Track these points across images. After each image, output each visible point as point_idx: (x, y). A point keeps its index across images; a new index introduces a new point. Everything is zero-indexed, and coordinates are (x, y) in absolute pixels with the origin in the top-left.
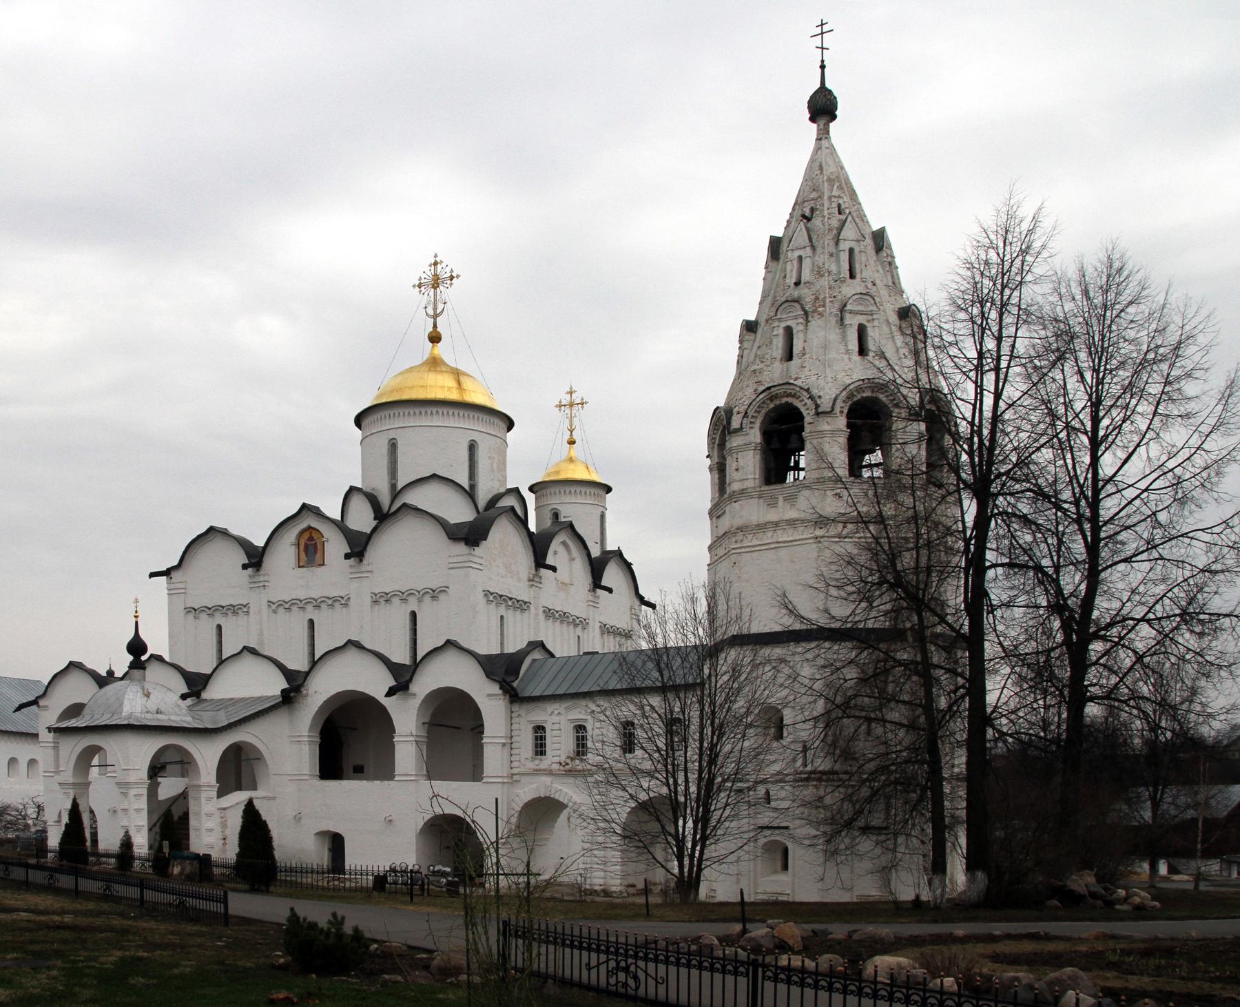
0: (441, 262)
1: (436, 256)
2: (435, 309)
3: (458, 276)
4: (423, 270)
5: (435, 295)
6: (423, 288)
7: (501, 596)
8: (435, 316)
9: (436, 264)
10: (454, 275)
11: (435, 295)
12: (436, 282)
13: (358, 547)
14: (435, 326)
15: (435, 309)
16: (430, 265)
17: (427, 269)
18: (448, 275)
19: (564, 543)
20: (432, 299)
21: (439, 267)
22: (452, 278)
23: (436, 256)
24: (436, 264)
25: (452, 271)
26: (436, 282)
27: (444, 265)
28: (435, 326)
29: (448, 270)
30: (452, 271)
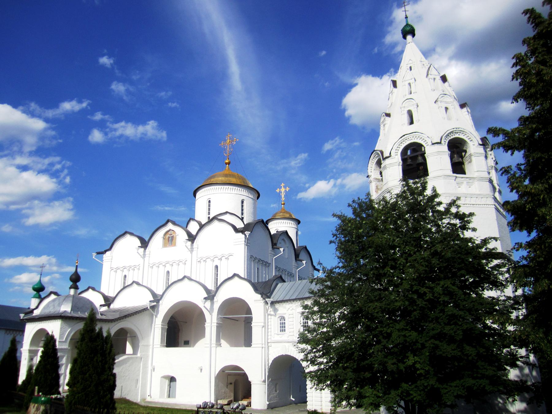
13: (192, 238)
19: (283, 239)
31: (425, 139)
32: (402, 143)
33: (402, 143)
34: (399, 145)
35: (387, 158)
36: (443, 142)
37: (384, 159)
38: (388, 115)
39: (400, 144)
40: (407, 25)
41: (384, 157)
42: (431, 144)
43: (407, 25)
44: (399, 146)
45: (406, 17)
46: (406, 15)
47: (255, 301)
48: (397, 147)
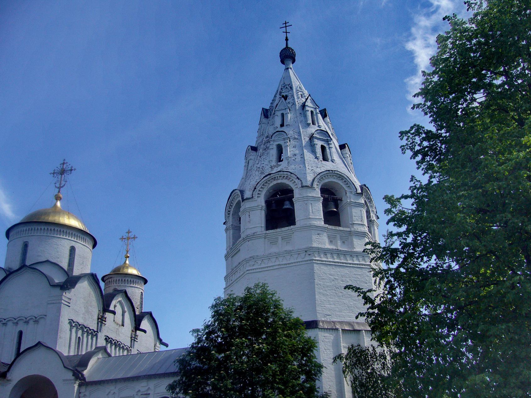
0: (67, 163)
1: (64, 160)
2: (60, 184)
3: (75, 169)
4: (57, 166)
5: (61, 177)
6: (55, 175)
7: (80, 325)
8: (60, 188)
9: (64, 164)
10: (73, 169)
11: (61, 177)
12: (63, 172)
14: (59, 192)
15: (60, 184)
16: (61, 164)
17: (59, 166)
18: (70, 168)
20: (60, 180)
21: (65, 166)
22: (71, 170)
23: (64, 160)
24: (64, 164)
25: (72, 167)
26: (63, 172)
27: (67, 164)
28: (59, 192)
29: (70, 166)
30: (72, 167)
31: (294, 180)
32: (266, 182)
33: (266, 182)
34: (263, 185)
35: (247, 199)
36: (315, 185)
37: (243, 200)
38: (254, 149)
39: (265, 184)
40: (287, 48)
41: (245, 198)
42: (300, 186)
43: (287, 48)
44: (263, 187)
45: (287, 40)
46: (287, 37)
47: (64, 380)
48: (260, 187)
